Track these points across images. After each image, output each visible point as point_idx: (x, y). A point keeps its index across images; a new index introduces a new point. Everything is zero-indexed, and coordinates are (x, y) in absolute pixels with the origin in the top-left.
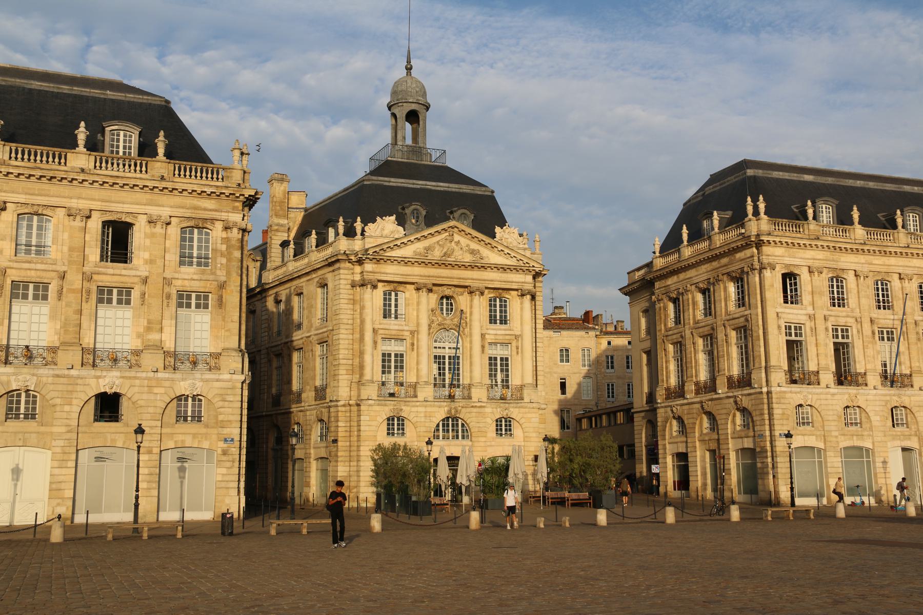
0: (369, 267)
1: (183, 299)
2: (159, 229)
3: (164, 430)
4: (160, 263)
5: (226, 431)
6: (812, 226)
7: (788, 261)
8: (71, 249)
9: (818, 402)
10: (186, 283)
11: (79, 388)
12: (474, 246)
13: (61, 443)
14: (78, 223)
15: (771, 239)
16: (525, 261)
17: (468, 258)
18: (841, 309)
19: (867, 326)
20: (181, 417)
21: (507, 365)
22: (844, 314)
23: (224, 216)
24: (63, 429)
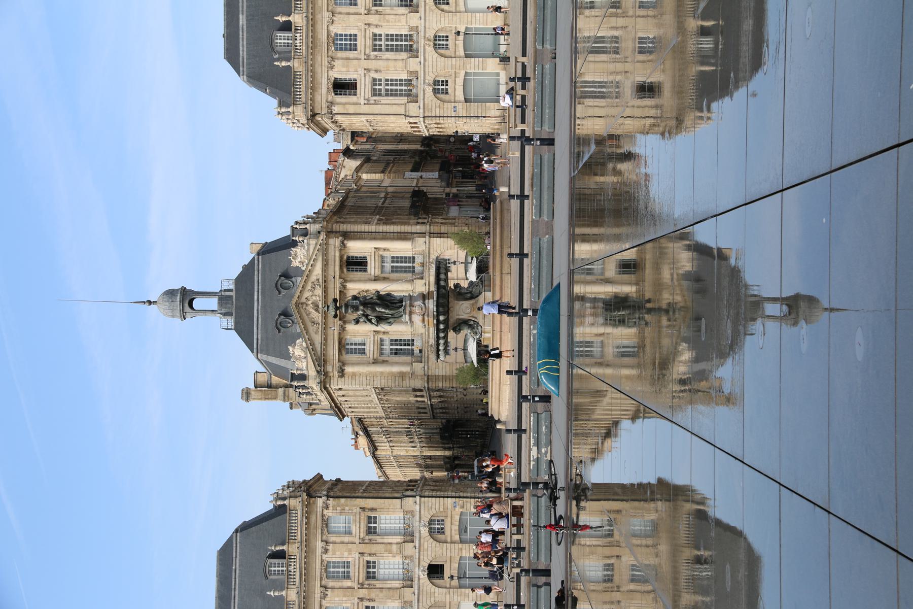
0: (329, 369)
1: (371, 531)
2: (330, 547)
3: (449, 540)
4: (350, 546)
5: (449, 507)
6: (297, 65)
7: (324, 90)
8: (345, 596)
9: (431, 74)
10: (362, 530)
11: (425, 589)
12: (309, 287)
13: (455, 597)
14: (329, 592)
15: (310, 108)
16: (318, 246)
17: (319, 291)
18: (358, 38)
19: (373, 19)
20: (441, 531)
21: (397, 258)
22: (363, 40)
23: (319, 510)
24: (448, 596)
